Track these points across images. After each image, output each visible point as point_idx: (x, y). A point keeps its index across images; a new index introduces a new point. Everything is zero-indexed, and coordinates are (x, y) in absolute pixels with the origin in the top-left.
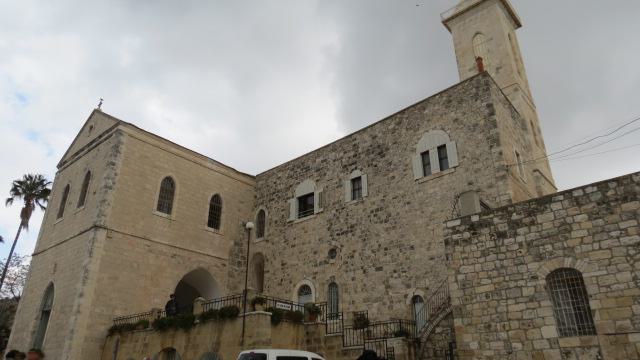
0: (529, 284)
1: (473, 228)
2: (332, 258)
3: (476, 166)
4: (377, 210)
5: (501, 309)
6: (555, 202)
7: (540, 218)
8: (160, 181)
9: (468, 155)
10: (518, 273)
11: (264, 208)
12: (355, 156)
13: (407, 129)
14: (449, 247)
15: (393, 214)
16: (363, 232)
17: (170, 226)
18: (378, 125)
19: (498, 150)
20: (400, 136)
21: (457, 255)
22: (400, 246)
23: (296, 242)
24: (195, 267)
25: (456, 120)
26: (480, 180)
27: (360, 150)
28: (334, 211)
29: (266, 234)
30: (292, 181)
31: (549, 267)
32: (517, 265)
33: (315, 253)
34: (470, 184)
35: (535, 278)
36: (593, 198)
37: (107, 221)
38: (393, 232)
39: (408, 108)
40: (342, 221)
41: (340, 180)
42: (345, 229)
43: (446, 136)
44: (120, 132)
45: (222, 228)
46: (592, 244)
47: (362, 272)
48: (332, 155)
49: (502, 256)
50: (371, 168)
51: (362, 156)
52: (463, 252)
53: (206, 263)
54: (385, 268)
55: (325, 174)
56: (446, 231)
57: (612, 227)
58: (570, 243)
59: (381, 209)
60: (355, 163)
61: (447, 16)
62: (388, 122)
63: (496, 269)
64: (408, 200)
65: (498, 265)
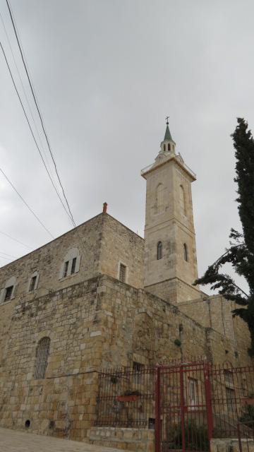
3: (86, 272)
5: (18, 362)
12: (38, 262)
30: (6, 277)
33: (5, 326)
35: (34, 342)
48: (28, 261)
52: (16, 325)
61: (145, 171)
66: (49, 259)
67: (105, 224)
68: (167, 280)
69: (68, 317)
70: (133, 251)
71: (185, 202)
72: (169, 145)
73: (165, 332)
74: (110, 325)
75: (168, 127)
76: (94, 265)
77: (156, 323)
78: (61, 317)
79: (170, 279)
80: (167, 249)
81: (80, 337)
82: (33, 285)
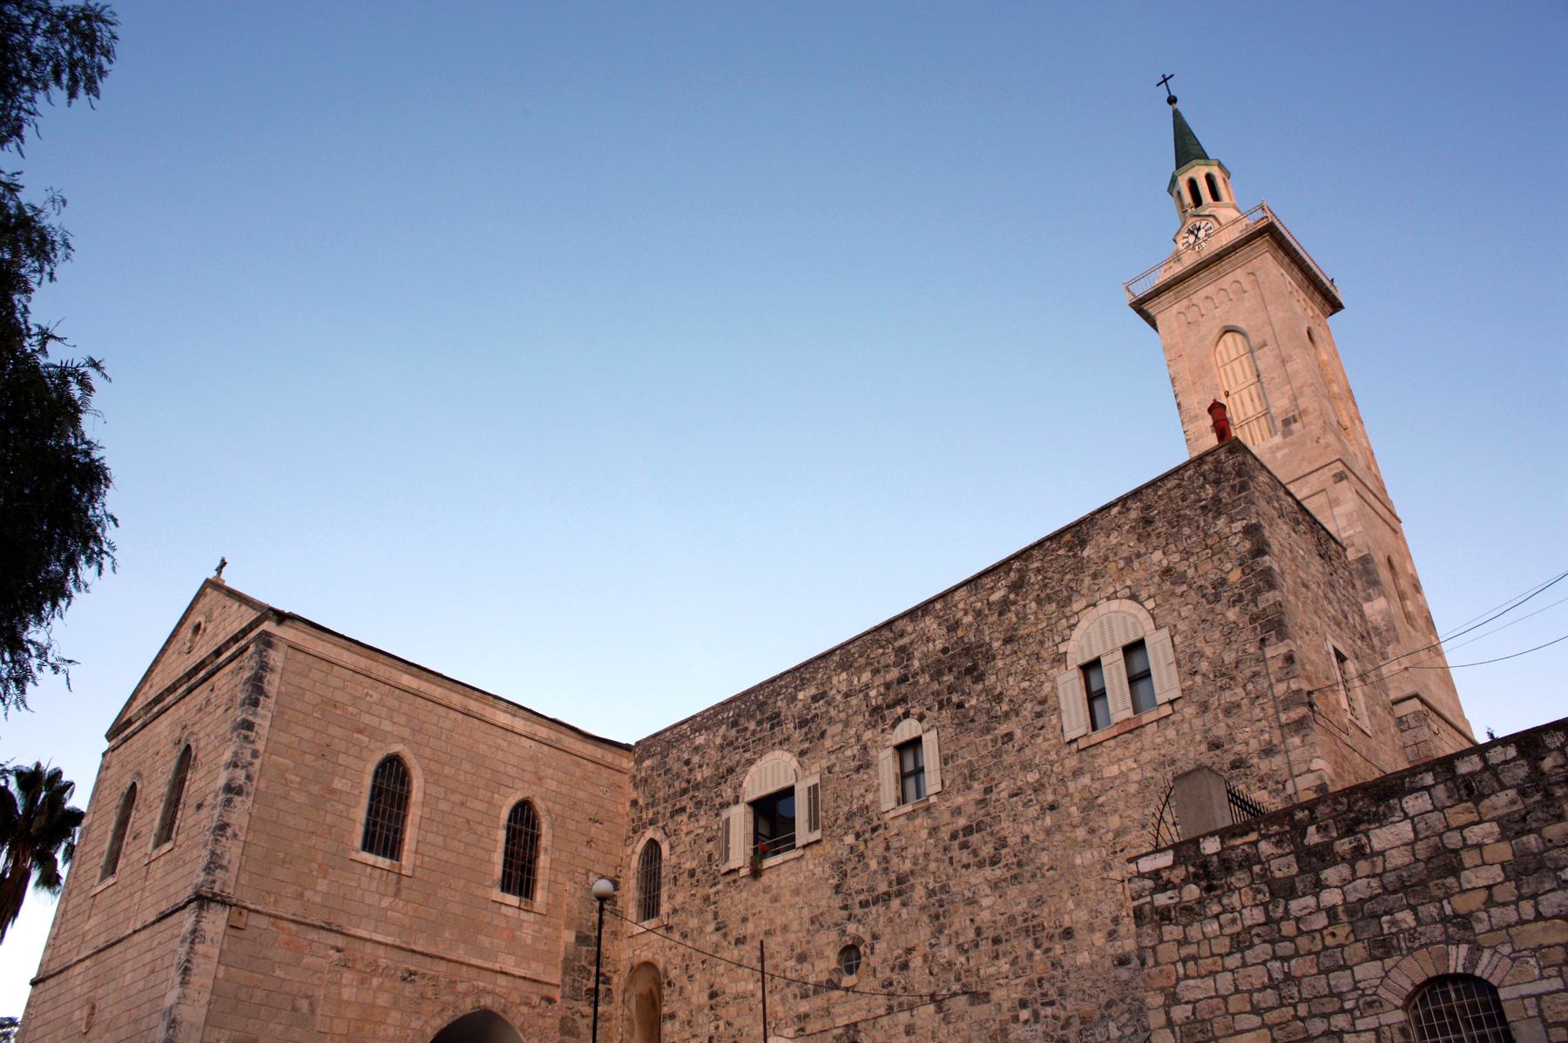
0: (1360, 1024)
1: (1210, 875)
2: (850, 970)
3: (1228, 696)
4: (968, 830)
7: (1380, 838)
8: (371, 768)
9: (1204, 666)
10: (1331, 994)
11: (659, 836)
12: (903, 679)
13: (1039, 601)
14: (1147, 929)
15: (1011, 840)
16: (931, 893)
17: (397, 894)
18: (962, 593)
19: (1282, 649)
20: (1022, 618)
21: (1168, 952)
22: (1032, 930)
23: (750, 928)
24: (467, 1006)
25: (1167, 572)
26: (1240, 737)
27: (916, 663)
28: (850, 839)
29: (665, 907)
31: (1410, 971)
32: (1327, 972)
33: (802, 958)
34: (1215, 745)
35: (1374, 1004)
36: (1506, 778)
37: (225, 882)
38: (1013, 891)
39: (1040, 544)
40: (873, 864)
41: (865, 748)
42: (883, 888)
43: (1143, 615)
44: (267, 641)
45: (540, 896)
46: (1516, 903)
47: (932, 1008)
48: (840, 681)
49: (1285, 948)
50: (946, 713)
51: (923, 679)
52: (1183, 942)
53: (495, 994)
54: (998, 994)
55: (823, 734)
56: (1137, 884)
58: (1462, 904)
59: (979, 827)
60: (904, 700)
61: (1141, 289)
62: (988, 582)
63: (1273, 984)
64: (1050, 798)
65: (1278, 975)
72: (1210, 179)
75: (1176, 114)
76: (1261, 660)
82: (910, 775)
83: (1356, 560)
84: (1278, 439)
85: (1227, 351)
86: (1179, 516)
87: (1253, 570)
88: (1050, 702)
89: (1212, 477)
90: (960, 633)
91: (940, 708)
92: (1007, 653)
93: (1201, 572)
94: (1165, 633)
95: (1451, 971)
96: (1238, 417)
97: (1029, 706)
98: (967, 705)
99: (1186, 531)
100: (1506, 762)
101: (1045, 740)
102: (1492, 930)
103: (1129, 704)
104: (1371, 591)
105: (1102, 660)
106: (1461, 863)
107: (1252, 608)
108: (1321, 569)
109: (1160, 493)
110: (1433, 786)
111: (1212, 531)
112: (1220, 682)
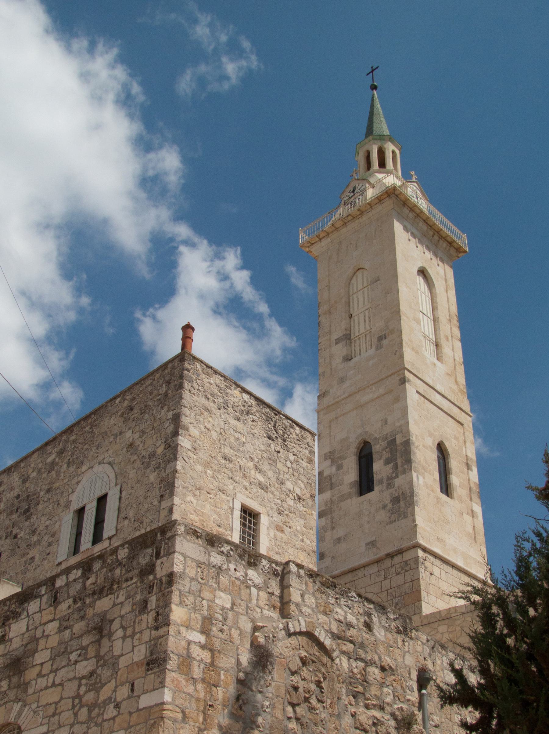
6: (36, 597)
9: (131, 514)
13: (69, 464)
18: (35, 456)
25: (131, 445)
39: (78, 423)
43: (112, 476)
46: (48, 675)
50: (8, 541)
57: (75, 644)
62: (49, 448)
66: (25, 506)
67: (187, 385)
68: (390, 556)
69: (73, 657)
70: (279, 465)
71: (436, 321)
72: (381, 153)
73: (374, 691)
74: (197, 672)
77: (344, 663)
78: (53, 659)
79: (400, 552)
80: (387, 462)
81: (111, 712)
83: (401, 444)
84: (372, 352)
85: (357, 283)
86: (146, 406)
87: (170, 446)
88: (56, 536)
89: (167, 378)
90: (27, 484)
91: (6, 538)
92: (45, 500)
93: (146, 447)
94: (118, 487)
95: (9, 721)
96: (354, 333)
97: (46, 538)
98: (19, 536)
99: (146, 416)
100: (75, 580)
101: (48, 563)
102: (34, 693)
103: (91, 539)
104: (406, 466)
105: (86, 509)
106: (37, 648)
107: (163, 474)
108: (262, 447)
109: (141, 389)
110: (43, 595)
111: (159, 417)
112: (137, 524)
